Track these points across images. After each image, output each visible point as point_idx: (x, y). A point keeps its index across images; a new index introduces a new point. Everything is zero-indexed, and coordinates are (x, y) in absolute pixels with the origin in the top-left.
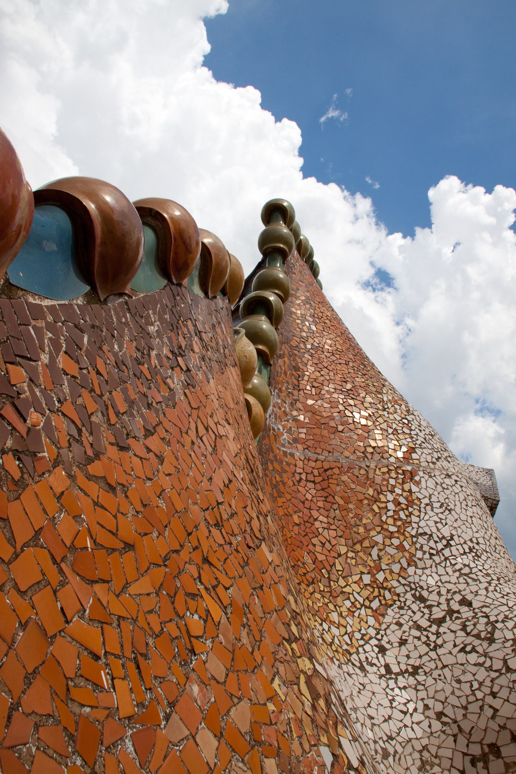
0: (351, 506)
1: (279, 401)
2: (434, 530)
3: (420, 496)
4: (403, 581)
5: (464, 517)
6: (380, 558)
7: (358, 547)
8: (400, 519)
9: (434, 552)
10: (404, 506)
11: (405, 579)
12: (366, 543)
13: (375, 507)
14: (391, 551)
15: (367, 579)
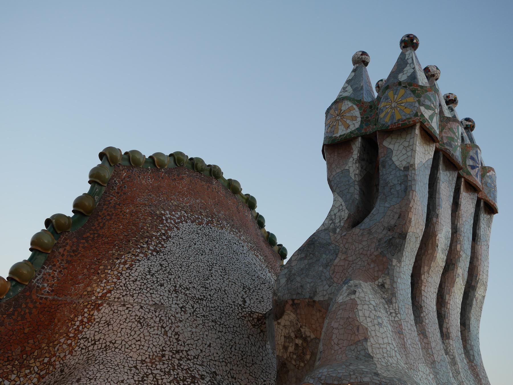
0: (59, 324)
1: (51, 271)
2: (92, 336)
3: (96, 317)
4: (62, 362)
5: (115, 329)
6: (58, 350)
7: (51, 345)
8: (79, 330)
9: (84, 347)
10: (84, 323)
11: (63, 360)
12: (56, 343)
13: (70, 325)
14: (65, 346)
15: (46, 360)
